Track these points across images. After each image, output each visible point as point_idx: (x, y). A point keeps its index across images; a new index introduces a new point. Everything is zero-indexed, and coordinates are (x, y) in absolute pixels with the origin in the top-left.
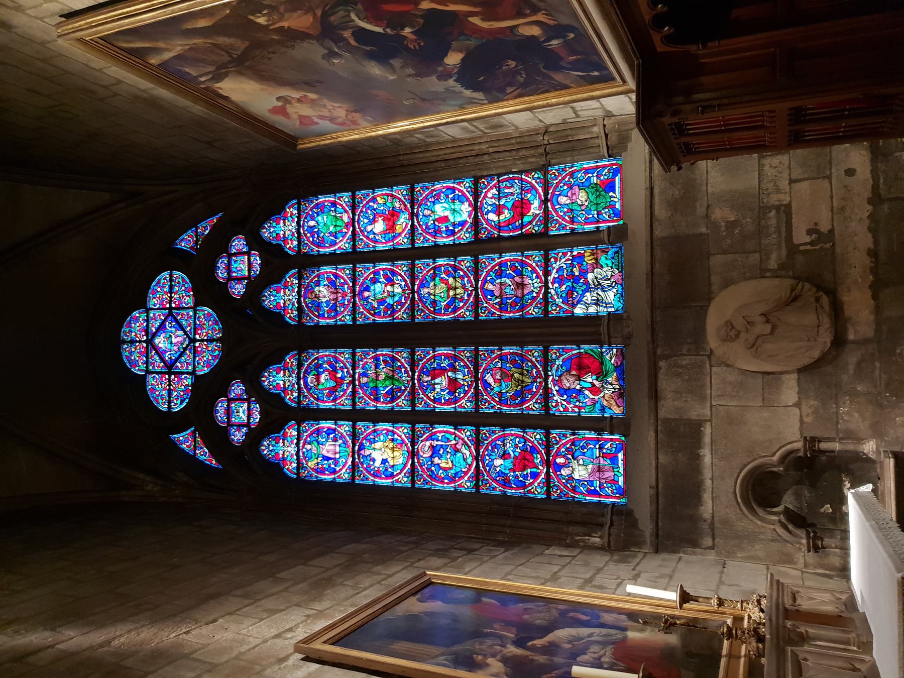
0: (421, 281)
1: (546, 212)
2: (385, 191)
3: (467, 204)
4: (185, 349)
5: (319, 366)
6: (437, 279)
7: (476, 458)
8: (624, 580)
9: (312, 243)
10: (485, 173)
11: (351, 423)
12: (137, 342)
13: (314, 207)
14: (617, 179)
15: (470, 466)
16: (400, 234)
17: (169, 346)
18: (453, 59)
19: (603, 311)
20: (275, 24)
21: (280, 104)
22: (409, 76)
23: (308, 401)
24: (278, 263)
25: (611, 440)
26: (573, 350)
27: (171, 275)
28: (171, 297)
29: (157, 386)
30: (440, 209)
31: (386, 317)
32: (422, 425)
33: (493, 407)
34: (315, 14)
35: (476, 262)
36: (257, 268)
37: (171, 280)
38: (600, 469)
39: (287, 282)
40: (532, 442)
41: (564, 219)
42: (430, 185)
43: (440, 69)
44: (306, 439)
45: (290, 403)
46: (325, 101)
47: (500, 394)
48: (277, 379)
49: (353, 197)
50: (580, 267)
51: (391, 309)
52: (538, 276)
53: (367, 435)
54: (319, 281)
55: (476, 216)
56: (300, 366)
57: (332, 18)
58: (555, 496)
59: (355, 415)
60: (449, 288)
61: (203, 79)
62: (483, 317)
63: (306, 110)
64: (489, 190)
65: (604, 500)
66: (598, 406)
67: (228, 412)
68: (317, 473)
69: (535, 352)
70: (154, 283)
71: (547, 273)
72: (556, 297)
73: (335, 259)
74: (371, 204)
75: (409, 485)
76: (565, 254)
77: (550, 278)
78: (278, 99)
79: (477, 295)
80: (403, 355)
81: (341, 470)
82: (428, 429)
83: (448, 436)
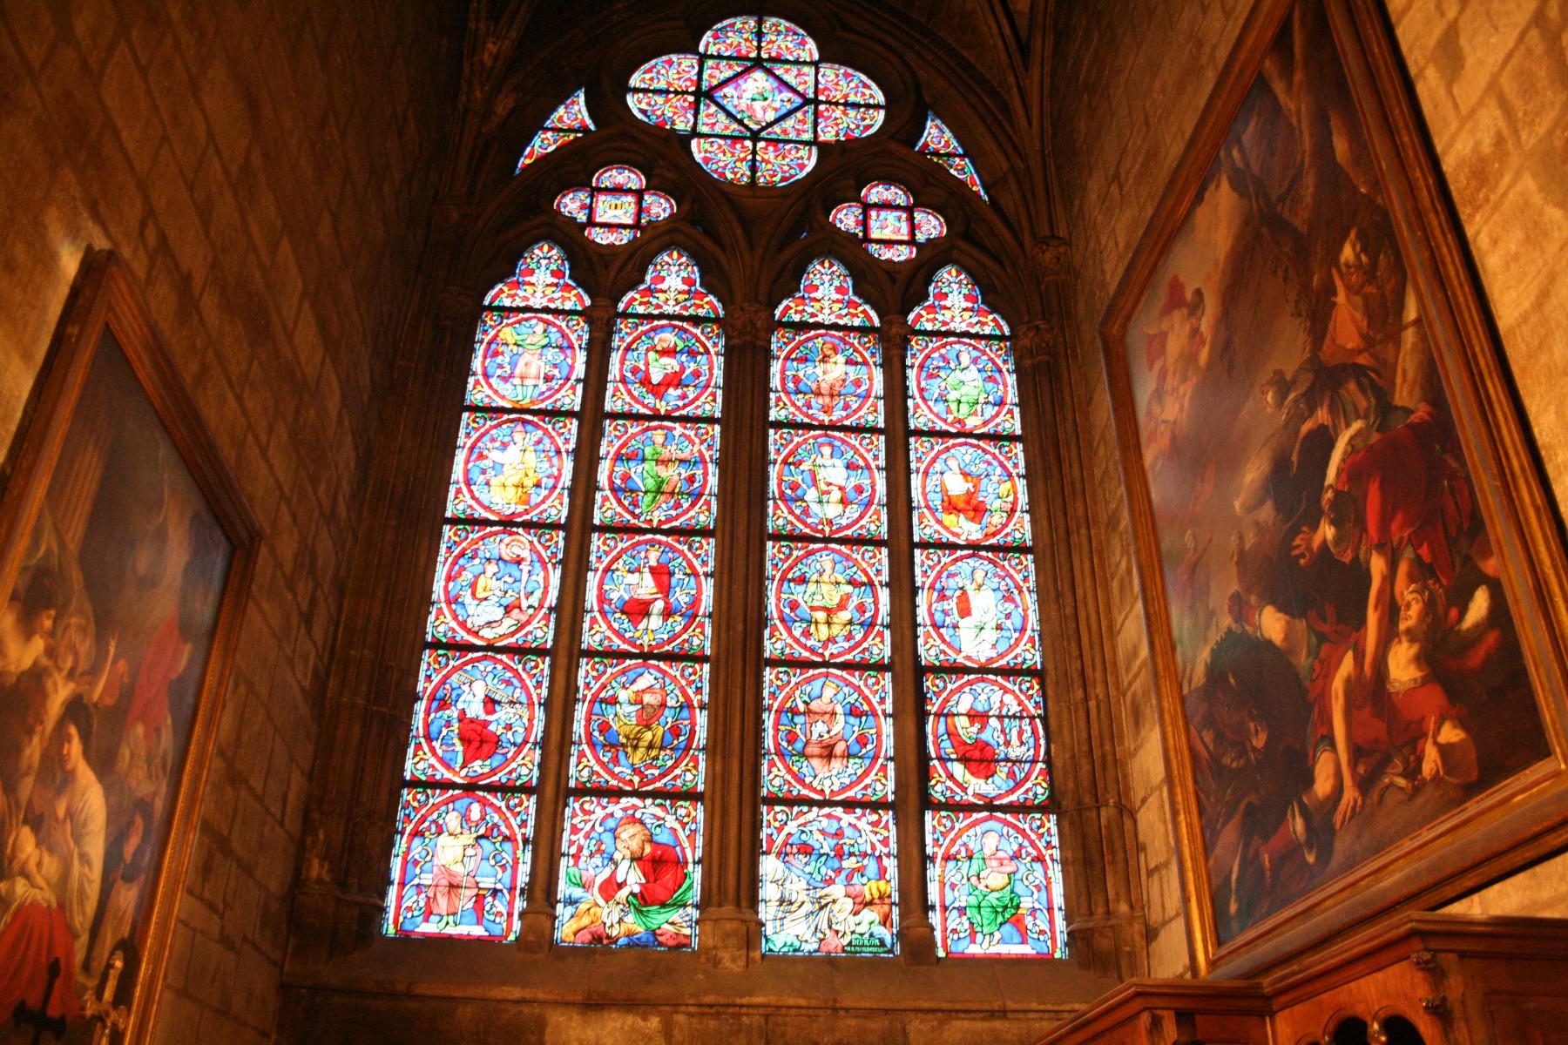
0: (848, 558)
1: (970, 808)
2: (1023, 499)
3: (993, 654)
4: (740, 122)
5: (692, 354)
6: (849, 589)
7: (490, 647)
8: (222, 917)
9: (928, 357)
10: (1050, 692)
11: (577, 408)
12: (760, 42)
13: (994, 363)
14: (1026, 950)
15: (476, 634)
16: (939, 522)
17: (747, 95)
18: (1272, 624)
19: (766, 912)
20: (1342, 278)
21: (1189, 296)
22: (1241, 538)
23: (624, 332)
24: (893, 293)
25: (510, 915)
26: (694, 849)
27: (877, 107)
28: (837, 104)
29: (675, 70)
30: (986, 604)
31: (779, 485)
32: (561, 544)
33: (587, 685)
34: (1360, 352)
35: (880, 667)
36: (887, 254)
37: (868, 106)
38: (453, 887)
39: (856, 306)
40: (513, 758)
41: (953, 841)
42: (1032, 584)
43: (1253, 599)
44: (554, 325)
45: (625, 299)
46: (1194, 380)
47: (613, 701)
48: (673, 277)
49: (1012, 438)
50: (858, 870)
51: (793, 496)
52: (844, 789)
53: (551, 437)
54: (856, 363)
55: (969, 671)
56: (696, 320)
57: (1352, 386)
58: (407, 795)
59: (592, 417)
60: (829, 611)
61: (1235, 153)
62: (769, 674)
63: (1175, 345)
64: (1017, 697)
65: (393, 892)
66: (577, 892)
67: (618, 190)
68: (489, 343)
69: (696, 776)
70: (864, 78)
71: (849, 805)
72: (801, 820)
73: (896, 395)
74: (999, 470)
75: (448, 514)
76: (885, 842)
77: (839, 811)
78: (1198, 293)
79: (815, 665)
80: (705, 515)
81: (490, 386)
82: (554, 555)
83: (538, 594)
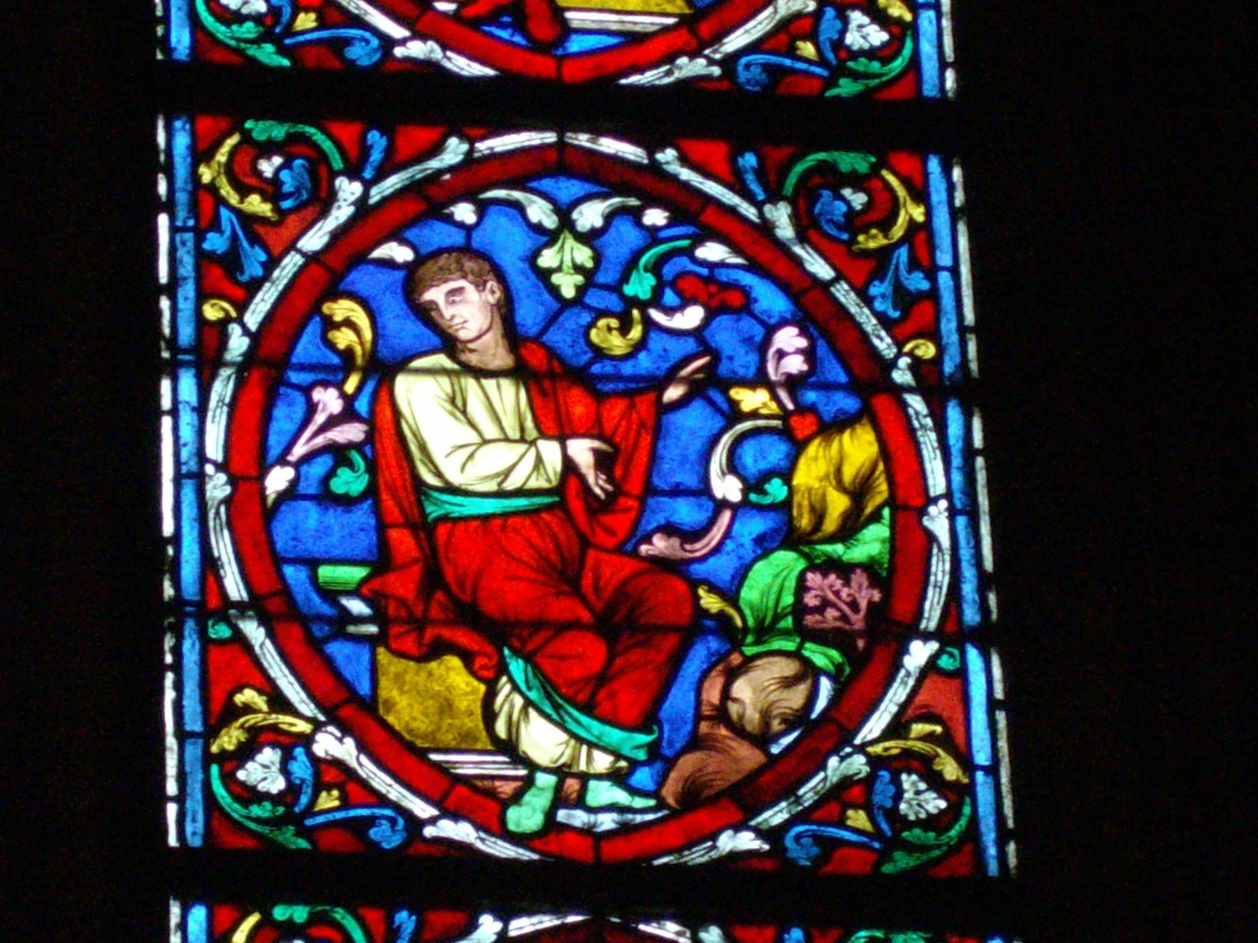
16: (352, 709)
49: (895, 122)
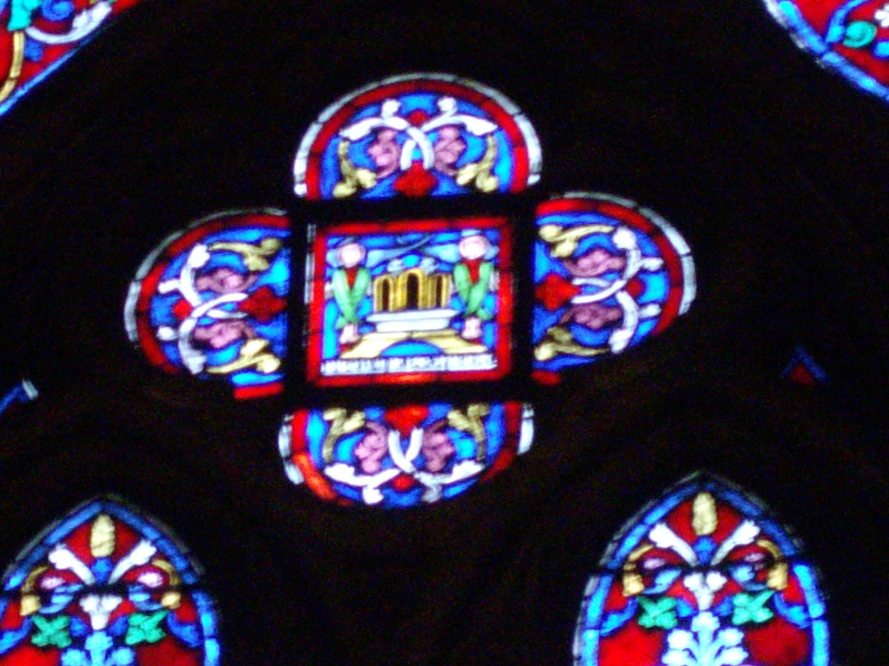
67: (416, 207)
